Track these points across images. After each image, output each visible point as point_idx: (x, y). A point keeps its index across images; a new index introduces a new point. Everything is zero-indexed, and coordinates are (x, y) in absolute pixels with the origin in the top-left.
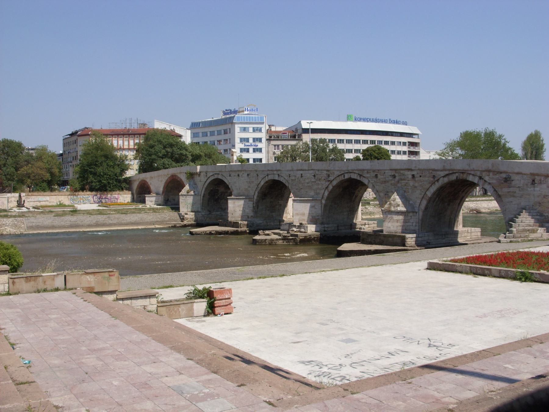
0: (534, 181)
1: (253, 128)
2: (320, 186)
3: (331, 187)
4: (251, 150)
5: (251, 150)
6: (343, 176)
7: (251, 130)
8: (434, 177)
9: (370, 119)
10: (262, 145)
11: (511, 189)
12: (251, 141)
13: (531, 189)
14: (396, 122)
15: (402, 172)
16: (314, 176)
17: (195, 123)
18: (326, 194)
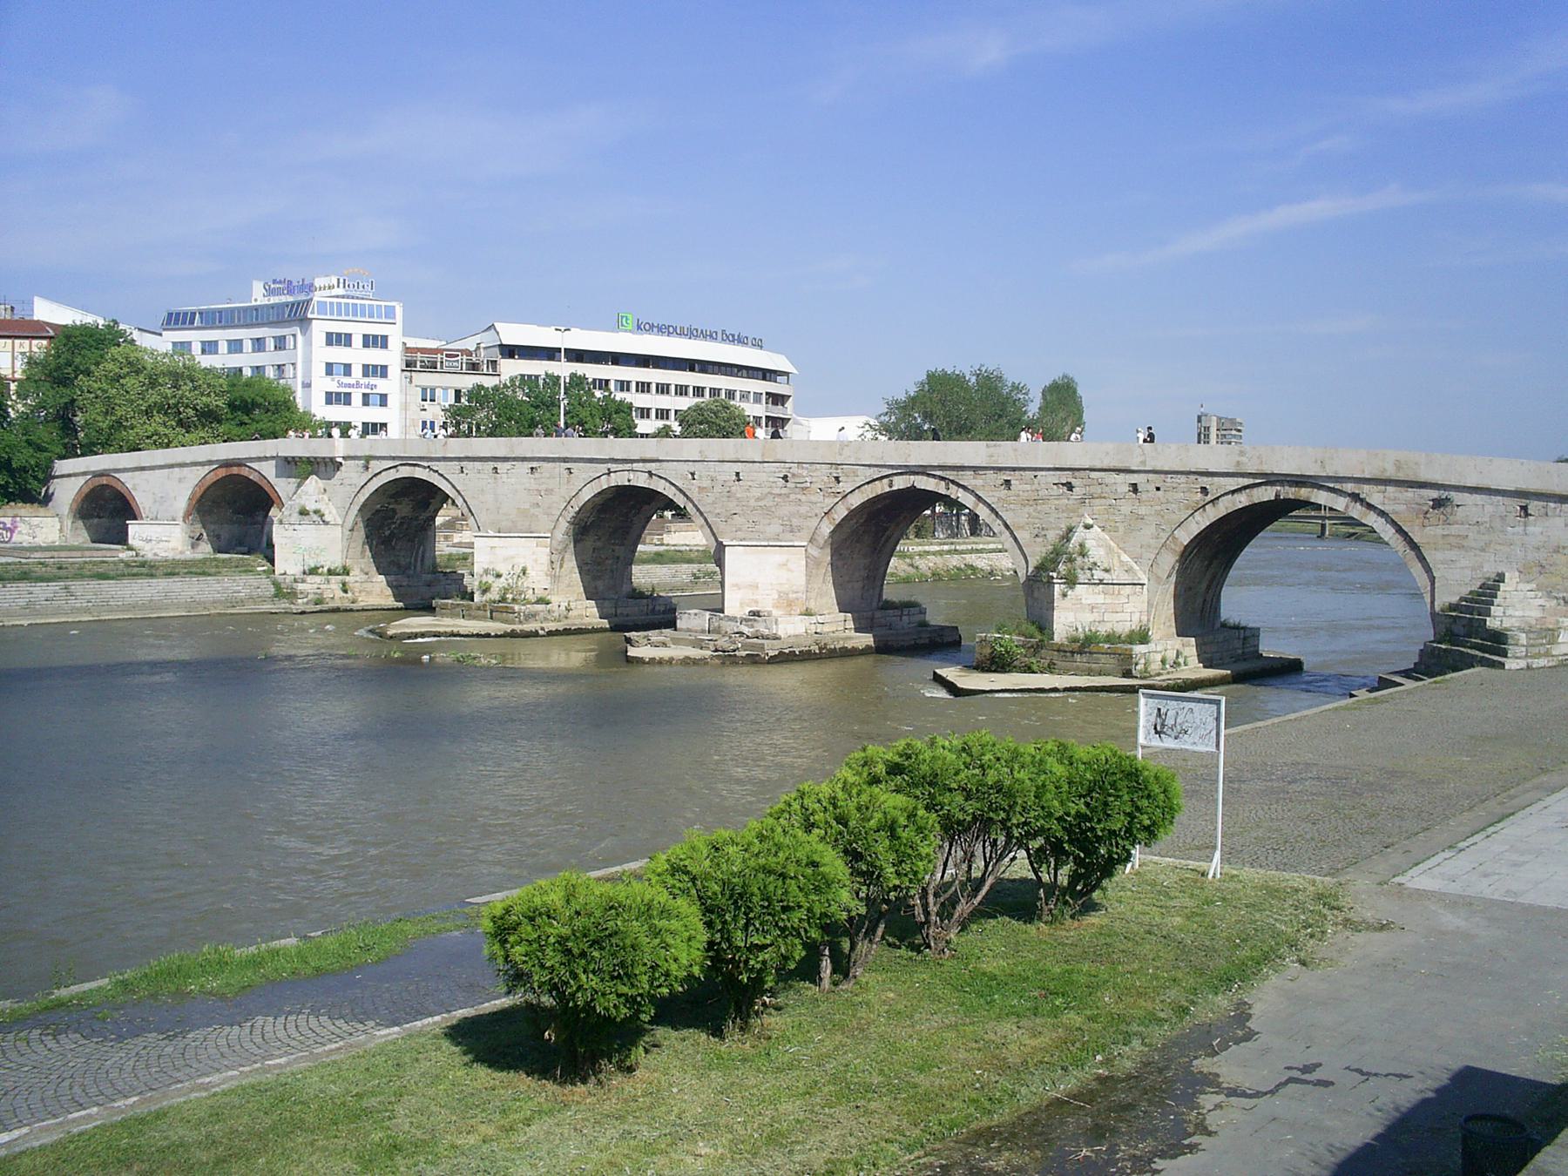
0: (1524, 508)
1: (366, 337)
2: (803, 509)
3: (841, 513)
4: (357, 398)
5: (357, 398)
6: (886, 481)
7: (357, 341)
8: (1204, 490)
9: (652, 326)
10: (391, 385)
11: (1454, 529)
12: (357, 371)
13: (1515, 530)
14: (740, 340)
15: (1093, 475)
16: (785, 478)
17: (178, 314)
18: (827, 529)
